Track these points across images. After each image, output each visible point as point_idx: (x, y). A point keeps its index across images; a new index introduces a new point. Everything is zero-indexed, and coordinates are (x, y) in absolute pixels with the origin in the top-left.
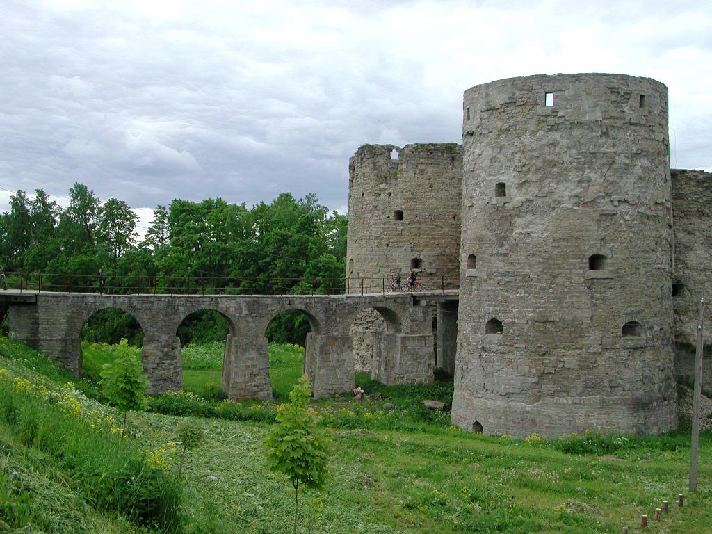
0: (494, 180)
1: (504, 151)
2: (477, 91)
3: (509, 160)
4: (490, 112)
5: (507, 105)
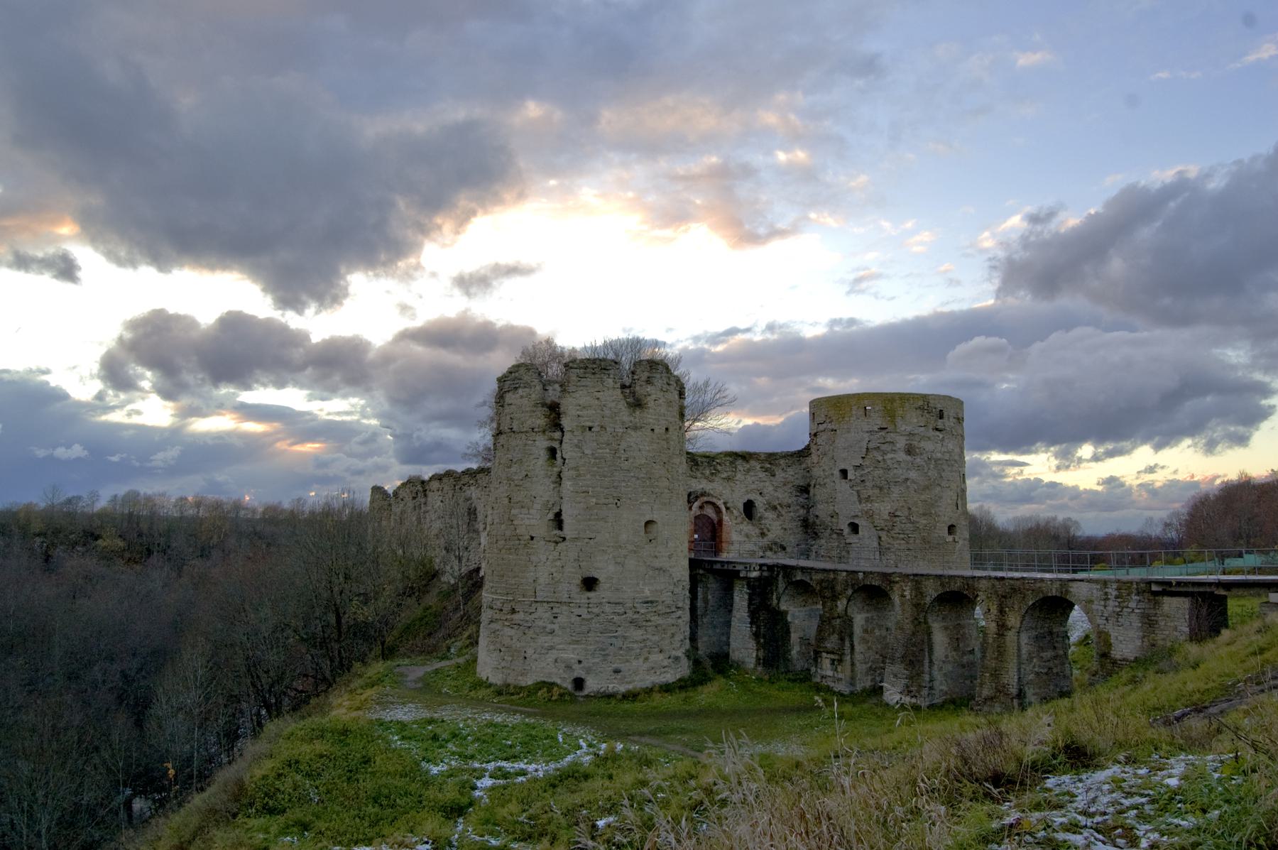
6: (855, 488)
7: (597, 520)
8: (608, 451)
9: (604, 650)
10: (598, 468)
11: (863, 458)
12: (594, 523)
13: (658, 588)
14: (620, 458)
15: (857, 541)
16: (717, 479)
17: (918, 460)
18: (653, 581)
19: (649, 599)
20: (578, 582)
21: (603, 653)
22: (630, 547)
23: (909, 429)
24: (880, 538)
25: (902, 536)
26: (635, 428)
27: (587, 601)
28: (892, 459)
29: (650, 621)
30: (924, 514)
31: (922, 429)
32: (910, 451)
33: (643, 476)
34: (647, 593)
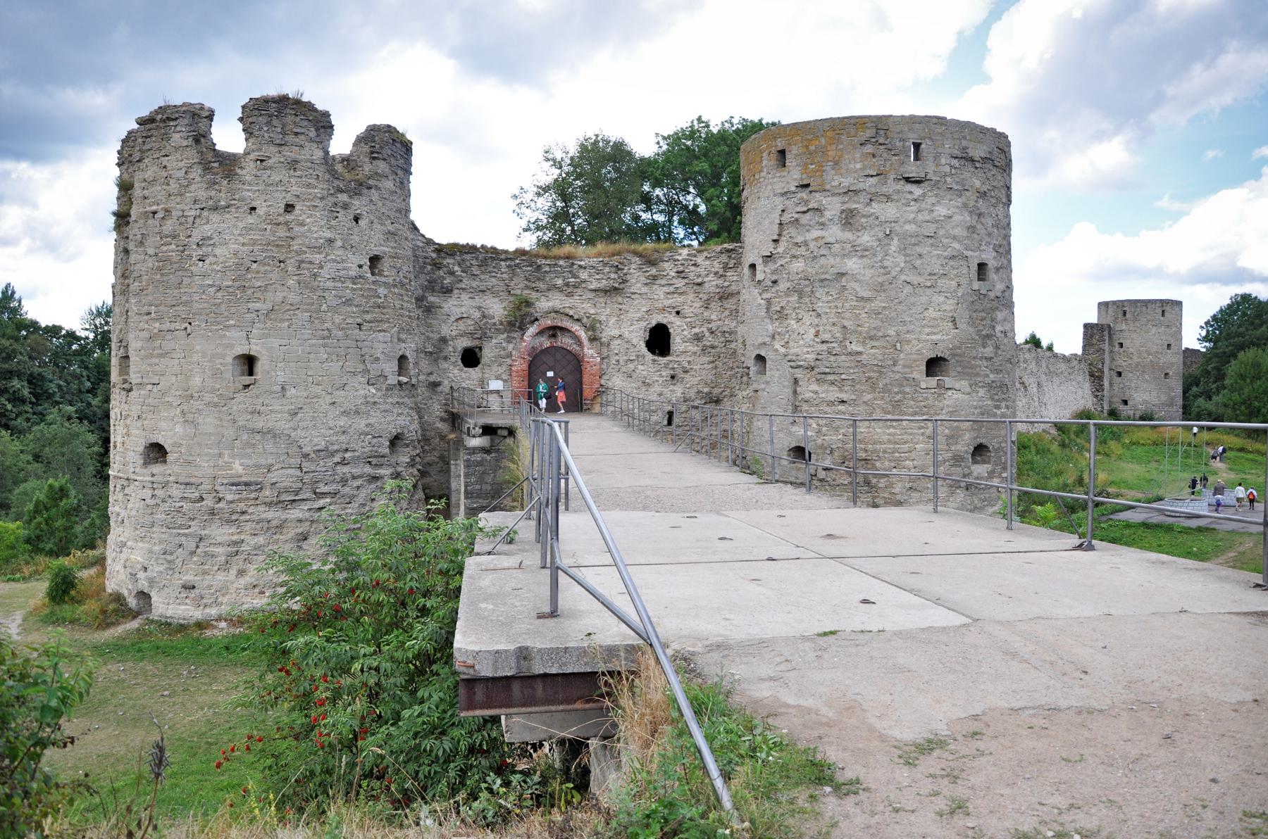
0: (975, 258)
1: (983, 220)
2: (942, 124)
4: (963, 162)
5: (985, 160)
6: (765, 296)
7: (161, 356)
8: (174, 246)
9: (171, 554)
10: (162, 275)
11: (774, 241)
12: (157, 361)
13: (263, 462)
14: (190, 256)
15: (763, 386)
16: (579, 291)
18: (250, 450)
19: (244, 479)
20: (141, 449)
21: (169, 558)
22: (208, 397)
23: (846, 182)
24: (796, 381)
26: (215, 209)
27: (151, 479)
28: (816, 239)
29: (243, 513)
32: (849, 219)
34: (238, 468)
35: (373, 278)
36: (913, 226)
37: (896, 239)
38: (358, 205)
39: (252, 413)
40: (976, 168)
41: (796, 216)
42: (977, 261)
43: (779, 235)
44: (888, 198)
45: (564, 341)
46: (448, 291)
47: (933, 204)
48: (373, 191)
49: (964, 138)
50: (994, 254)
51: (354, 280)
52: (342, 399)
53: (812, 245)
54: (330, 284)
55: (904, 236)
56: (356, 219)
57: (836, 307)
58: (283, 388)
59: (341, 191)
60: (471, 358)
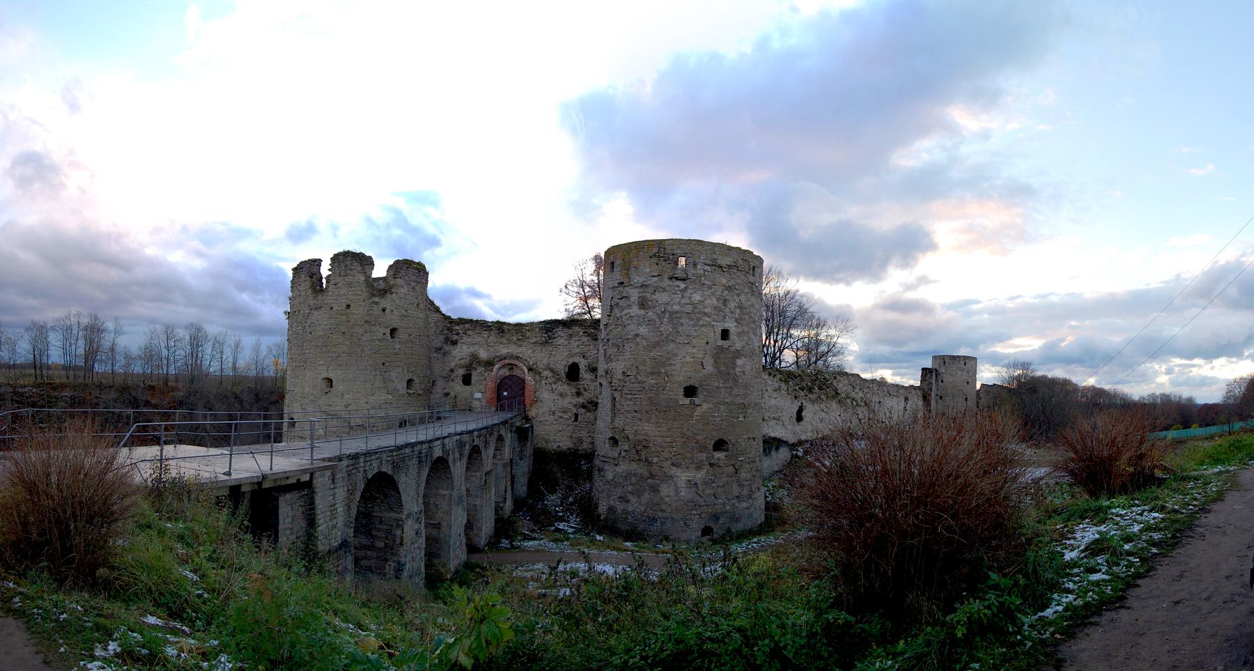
2: (699, 245)
3: (732, 312)
4: (714, 268)
5: (729, 267)
11: (608, 315)
16: (525, 344)
17: (651, 314)
22: (311, 397)
23: (641, 280)
25: (630, 396)
30: (652, 374)
31: (656, 279)
32: (643, 304)
33: (320, 344)
35: (392, 340)
36: (678, 306)
37: (667, 314)
38: (384, 303)
39: (328, 406)
40: (724, 272)
41: (617, 301)
42: (721, 328)
43: (611, 312)
44: (664, 290)
45: (517, 372)
46: (455, 343)
47: (692, 294)
48: (394, 295)
49: (715, 253)
50: (736, 324)
51: (380, 341)
52: (372, 401)
53: (624, 317)
54: (367, 343)
55: (671, 313)
56: (384, 310)
57: (634, 354)
58: (342, 395)
59: (375, 296)
60: (467, 380)
